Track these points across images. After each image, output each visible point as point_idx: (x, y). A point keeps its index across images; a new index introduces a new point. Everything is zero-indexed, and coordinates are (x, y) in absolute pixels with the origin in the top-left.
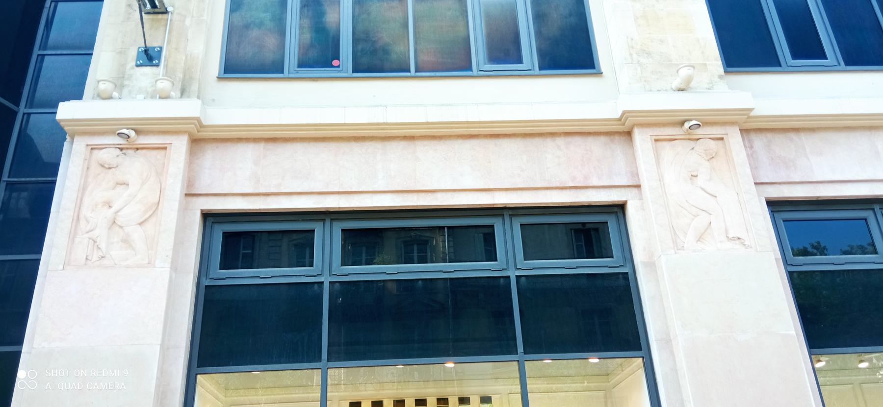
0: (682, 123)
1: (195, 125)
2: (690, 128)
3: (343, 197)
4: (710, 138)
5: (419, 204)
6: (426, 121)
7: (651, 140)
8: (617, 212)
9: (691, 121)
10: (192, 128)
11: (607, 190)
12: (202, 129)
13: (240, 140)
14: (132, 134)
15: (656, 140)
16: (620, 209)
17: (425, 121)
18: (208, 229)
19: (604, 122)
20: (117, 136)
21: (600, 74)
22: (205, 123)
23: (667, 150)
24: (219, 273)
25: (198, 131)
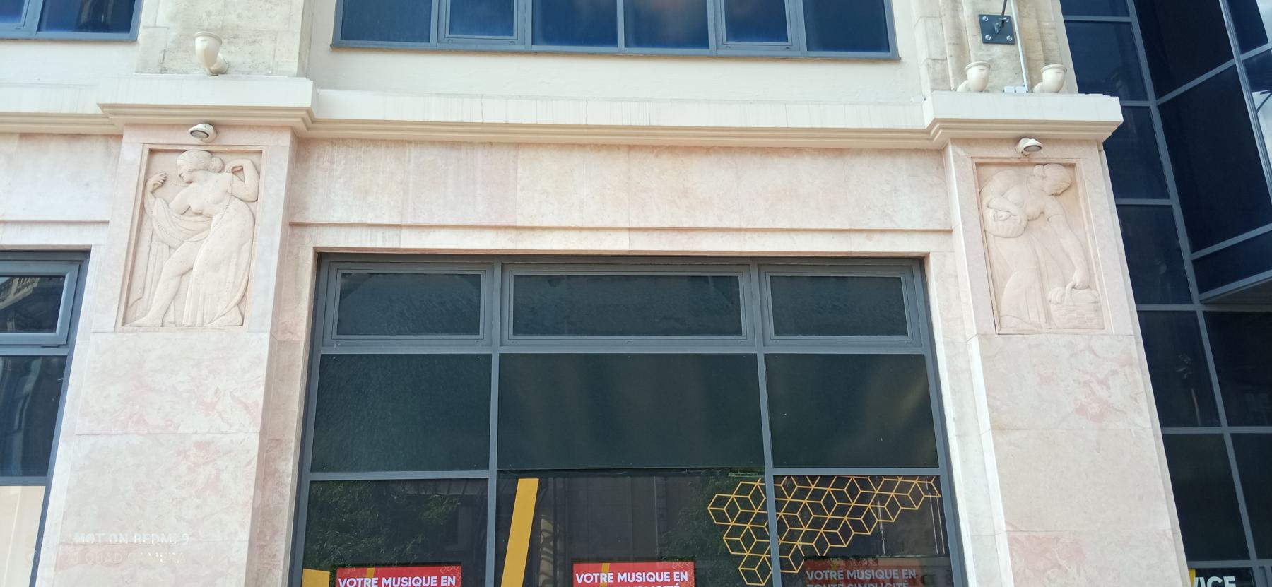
0: (1017, 140)
1: (303, 119)
2: (1025, 149)
3: (73, 229)
4: (1060, 164)
5: (567, 248)
6: (535, 123)
7: (972, 163)
8: (749, 265)
9: (1030, 138)
10: (297, 122)
11: (563, 232)
12: (314, 125)
13: (374, 142)
14: (209, 129)
15: (979, 165)
16: (918, 263)
17: (421, 120)
18: (324, 271)
19: (889, 134)
20: (190, 135)
21: (895, 59)
22: (317, 116)
23: (998, 180)
24: (60, 332)
25: (308, 129)
